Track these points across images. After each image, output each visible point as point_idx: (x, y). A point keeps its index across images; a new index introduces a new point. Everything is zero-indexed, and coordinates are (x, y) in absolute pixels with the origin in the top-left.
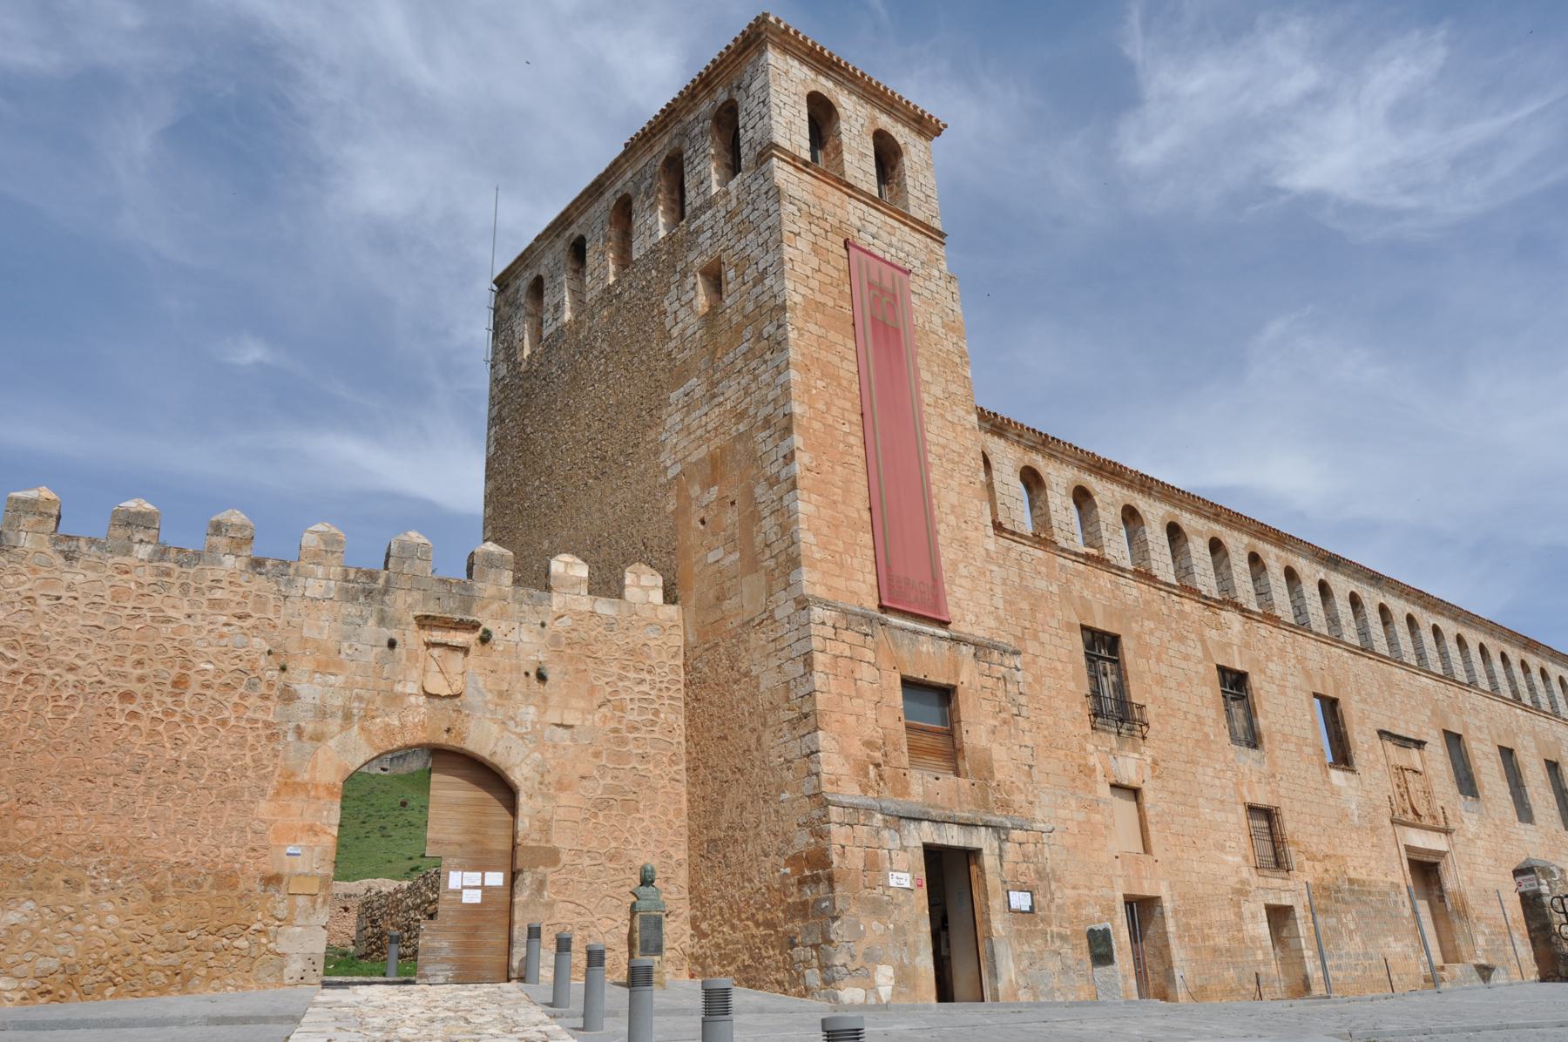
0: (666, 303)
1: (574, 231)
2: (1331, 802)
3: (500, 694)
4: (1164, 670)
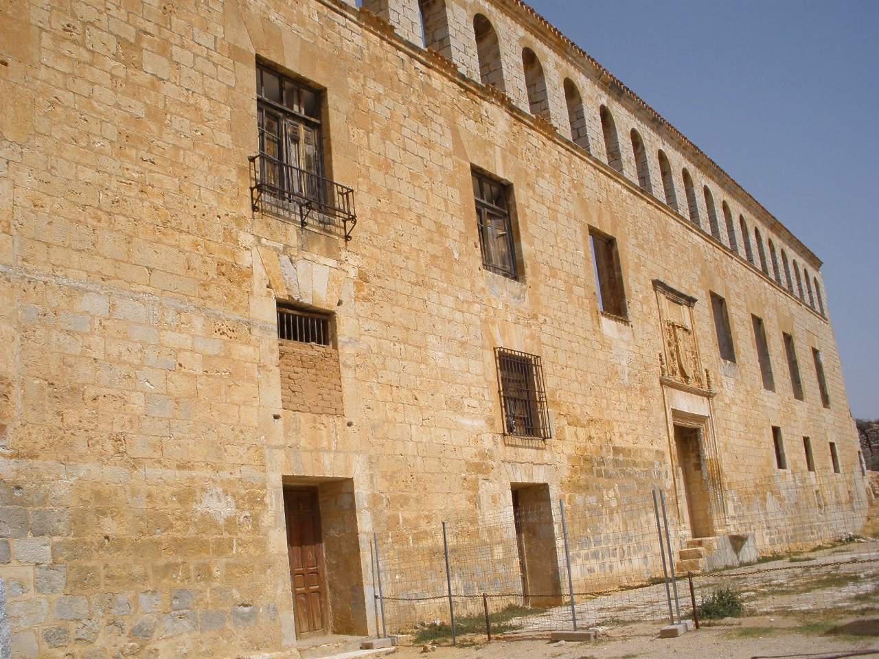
2: (601, 355)
4: (393, 152)
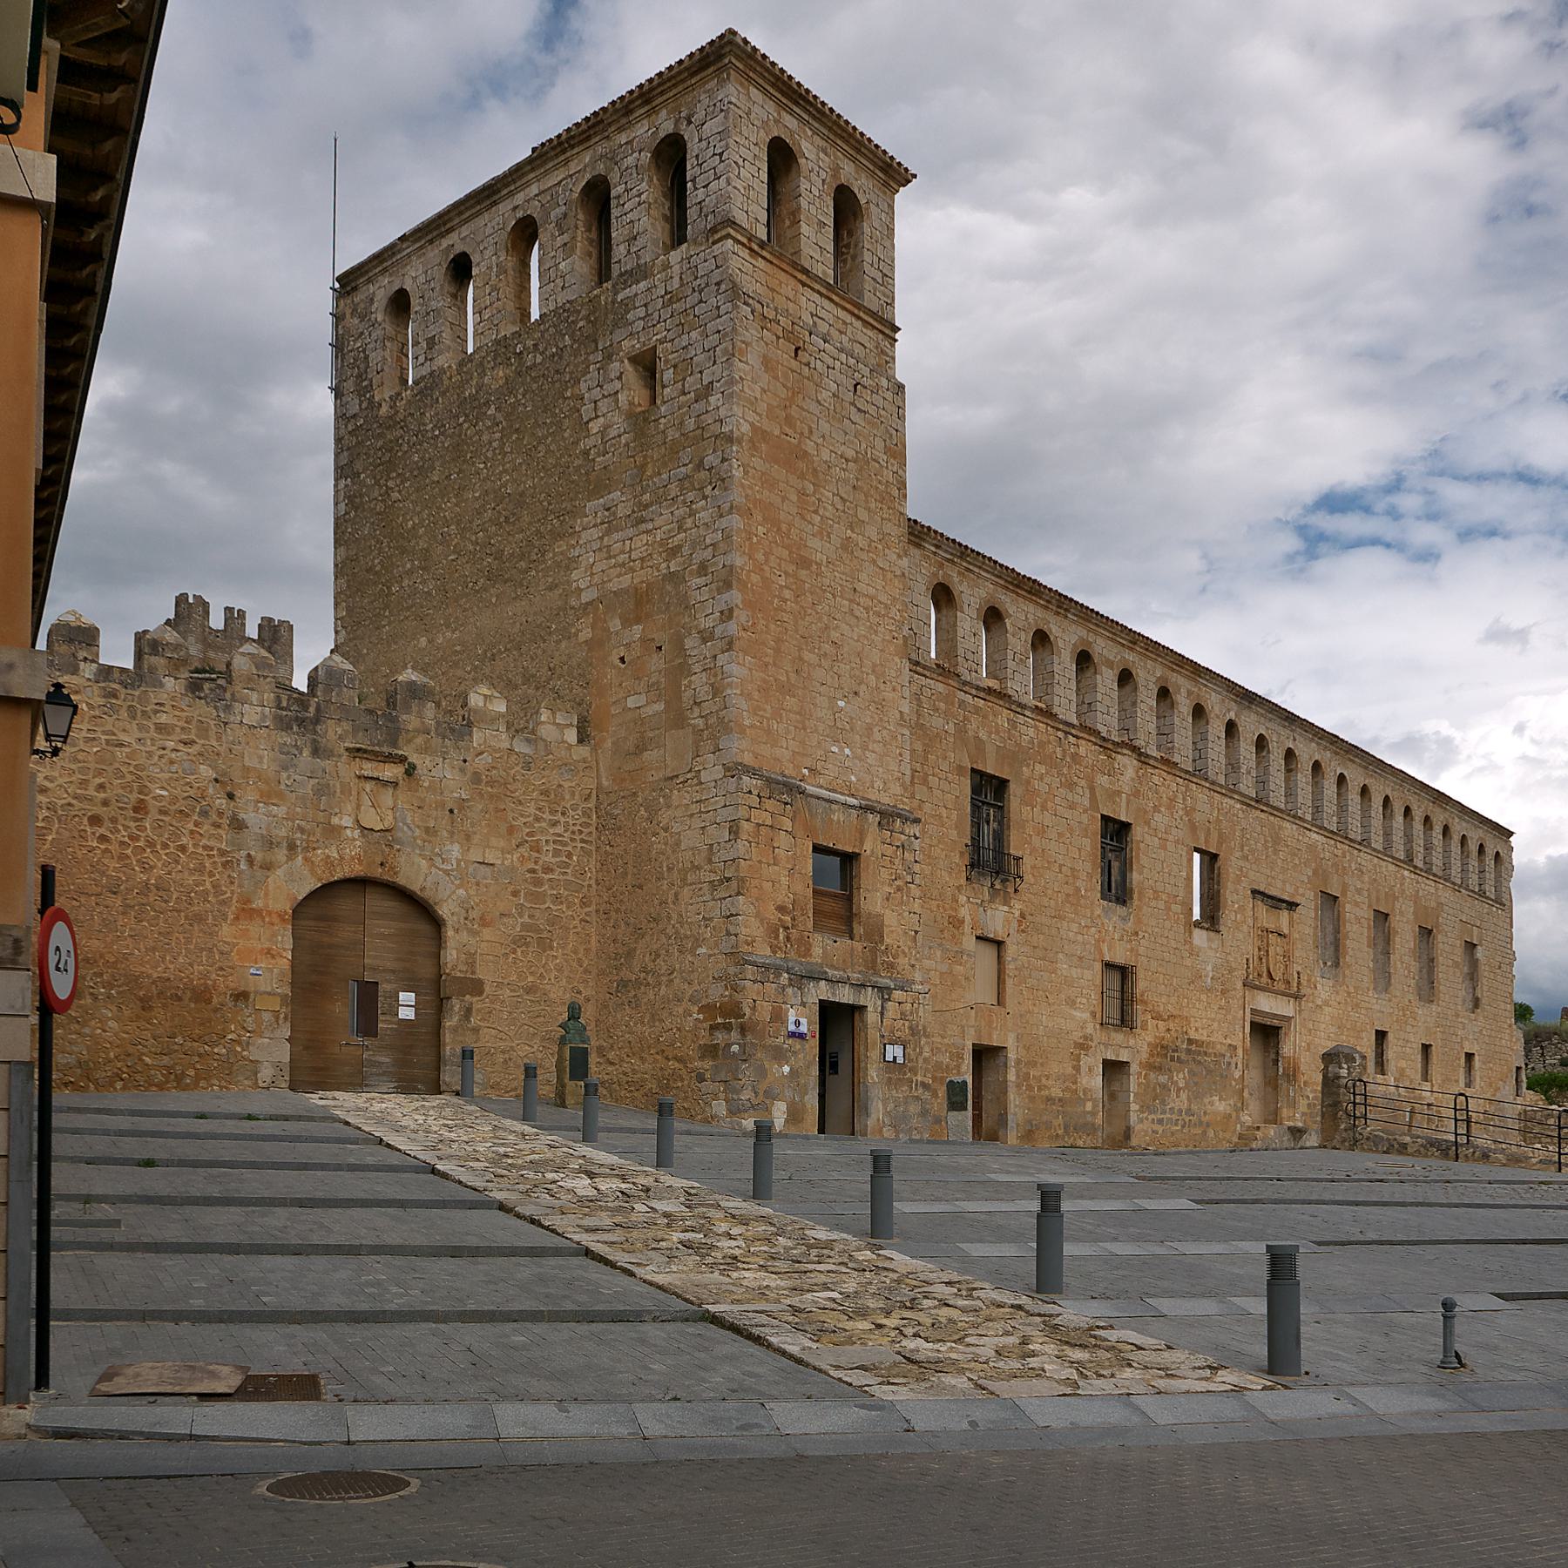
0: (583, 386)
1: (455, 242)
3: (427, 830)
